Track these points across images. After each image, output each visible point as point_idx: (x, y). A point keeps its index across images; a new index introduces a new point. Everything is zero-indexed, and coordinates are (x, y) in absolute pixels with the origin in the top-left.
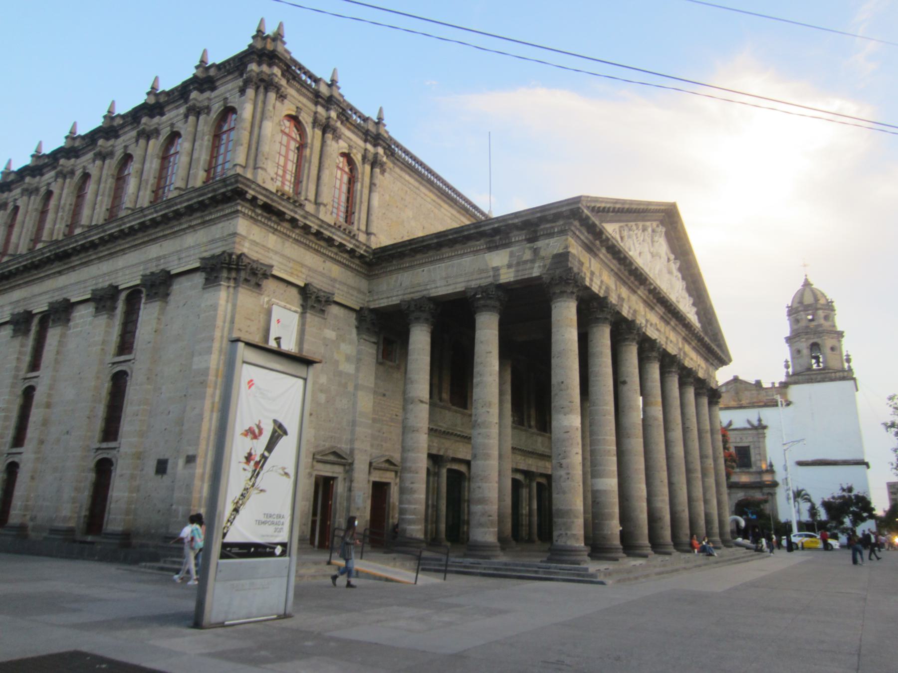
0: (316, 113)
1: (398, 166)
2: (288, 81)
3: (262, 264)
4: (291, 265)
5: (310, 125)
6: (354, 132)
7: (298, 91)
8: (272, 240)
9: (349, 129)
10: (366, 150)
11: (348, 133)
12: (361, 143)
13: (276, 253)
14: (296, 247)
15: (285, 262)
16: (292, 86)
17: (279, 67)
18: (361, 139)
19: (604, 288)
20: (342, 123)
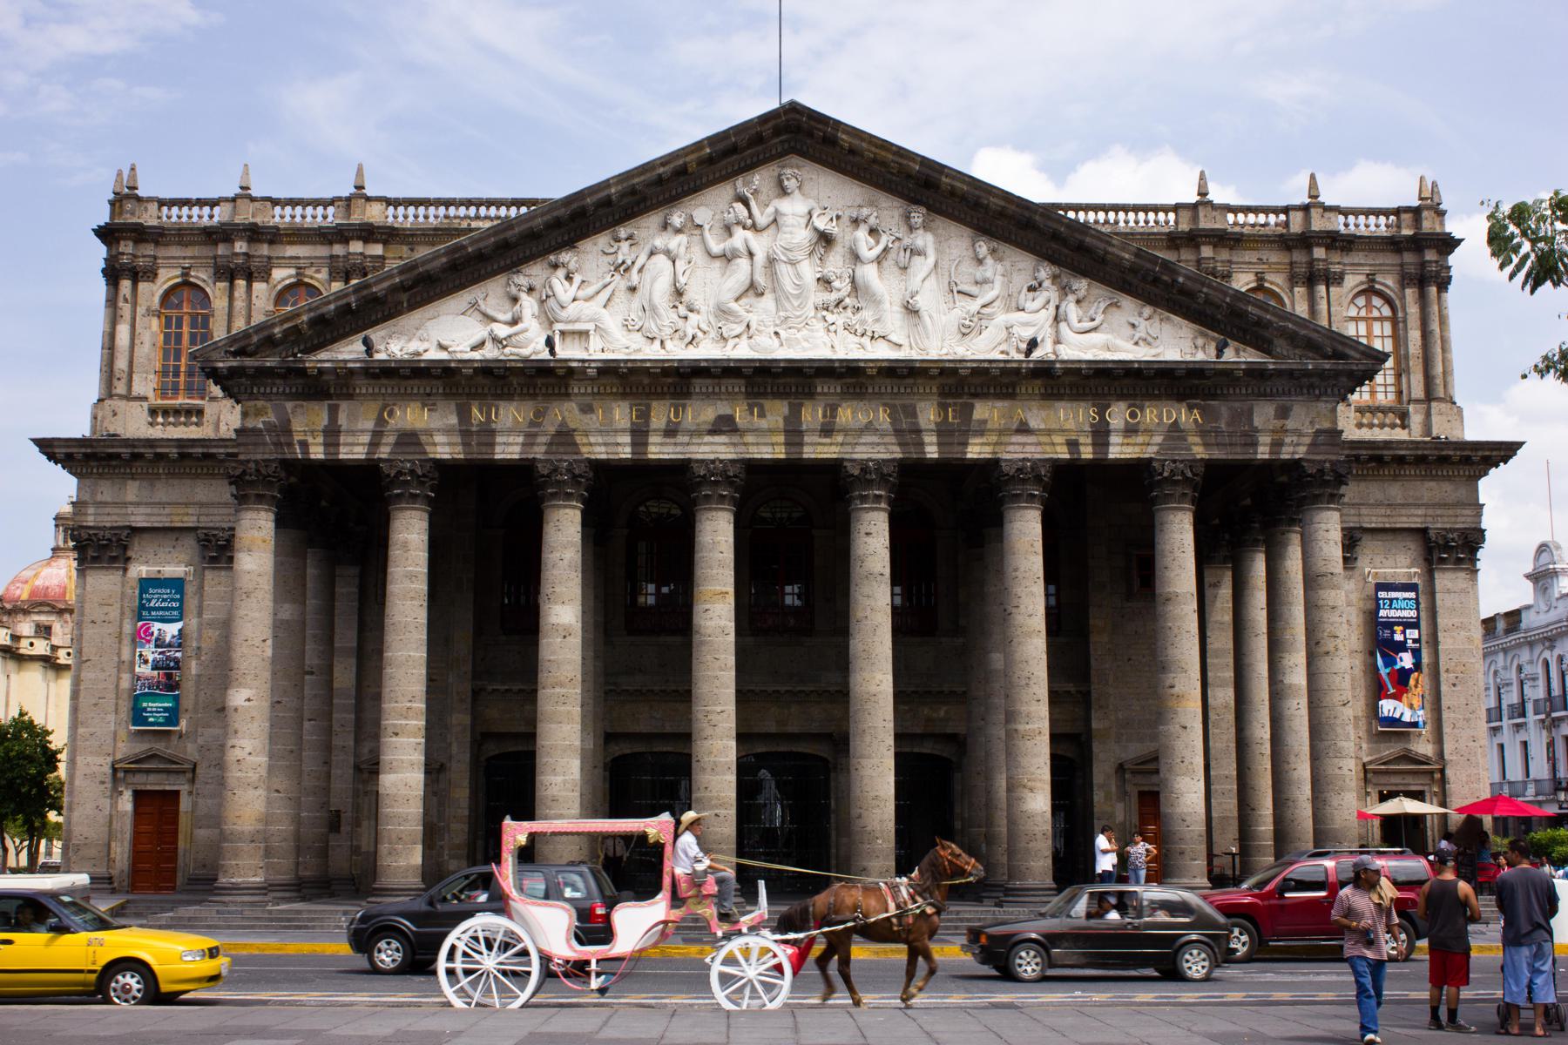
0: (215, 257)
1: (419, 243)
2: (157, 243)
3: (112, 528)
4: (167, 511)
5: (210, 282)
6: (302, 243)
7: (180, 243)
8: (132, 491)
9: (291, 243)
10: (332, 257)
11: (291, 251)
12: (322, 251)
13: (138, 504)
14: (176, 482)
15: (156, 511)
16: (166, 245)
17: (125, 239)
18: (322, 244)
19: (391, 439)
20: (271, 242)
